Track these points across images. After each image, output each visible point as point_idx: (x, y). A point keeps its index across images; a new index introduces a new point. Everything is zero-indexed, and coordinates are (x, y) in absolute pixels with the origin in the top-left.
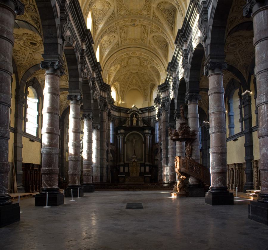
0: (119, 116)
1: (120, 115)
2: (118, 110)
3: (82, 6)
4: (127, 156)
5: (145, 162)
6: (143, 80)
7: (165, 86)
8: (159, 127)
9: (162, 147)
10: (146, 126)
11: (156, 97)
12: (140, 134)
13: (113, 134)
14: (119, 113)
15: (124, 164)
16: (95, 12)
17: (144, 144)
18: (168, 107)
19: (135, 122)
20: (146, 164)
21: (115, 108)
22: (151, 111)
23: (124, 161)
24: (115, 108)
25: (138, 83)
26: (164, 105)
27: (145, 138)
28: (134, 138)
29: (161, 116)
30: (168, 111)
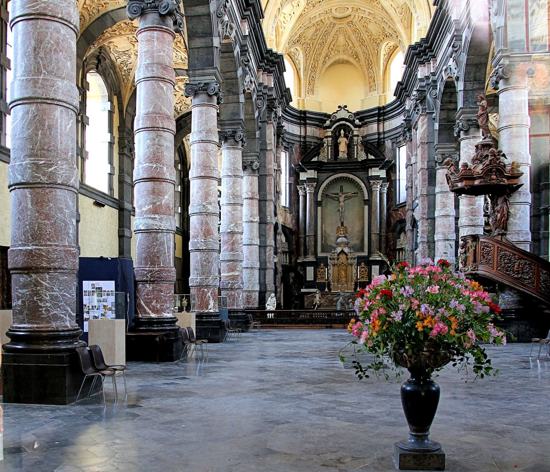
0: (303, 134)
1: (306, 133)
2: (300, 120)
6: (365, 36)
7: (426, 48)
8: (409, 159)
9: (417, 215)
10: (373, 157)
11: (400, 80)
14: (303, 129)
18: (435, 103)
19: (343, 148)
21: (293, 116)
22: (385, 117)
24: (293, 116)
25: (351, 45)
26: (425, 98)
28: (341, 190)
29: (413, 130)
30: (434, 115)
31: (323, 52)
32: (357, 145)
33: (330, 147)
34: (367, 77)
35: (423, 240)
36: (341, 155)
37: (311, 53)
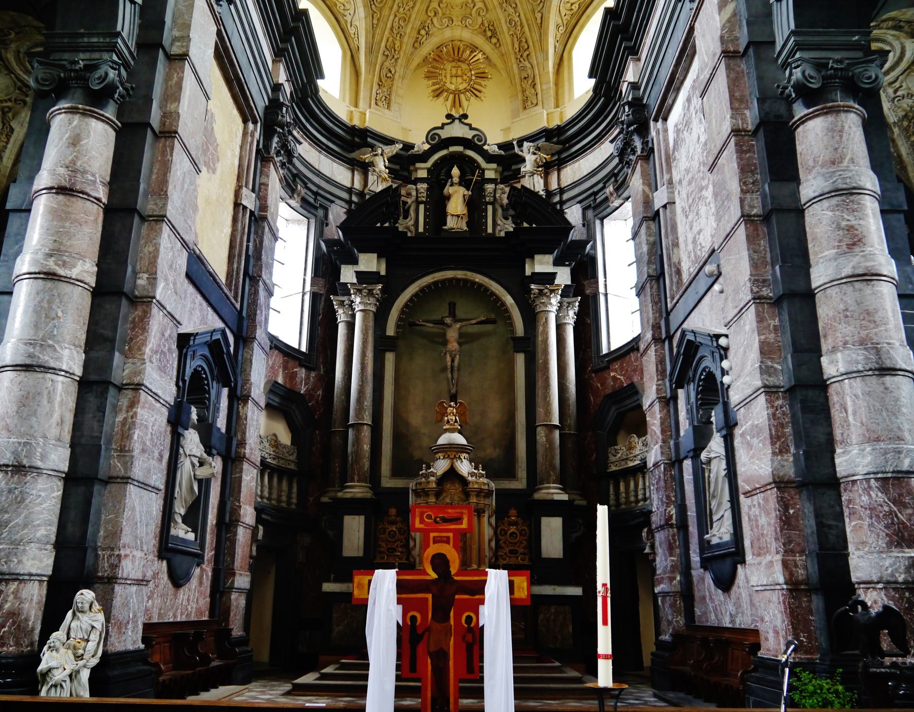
4: (399, 437)
5: (534, 481)
12: (496, 288)
13: (308, 288)
14: (358, 178)
15: (369, 495)
17: (520, 359)
20: (540, 495)
23: (374, 477)
24: (331, 134)
27: (534, 310)
28: (452, 314)
29: (655, 128)
31: (413, 16)
32: (492, 203)
33: (422, 207)
34: (518, 80)
35: (772, 381)
36: (451, 223)
37: (386, 12)
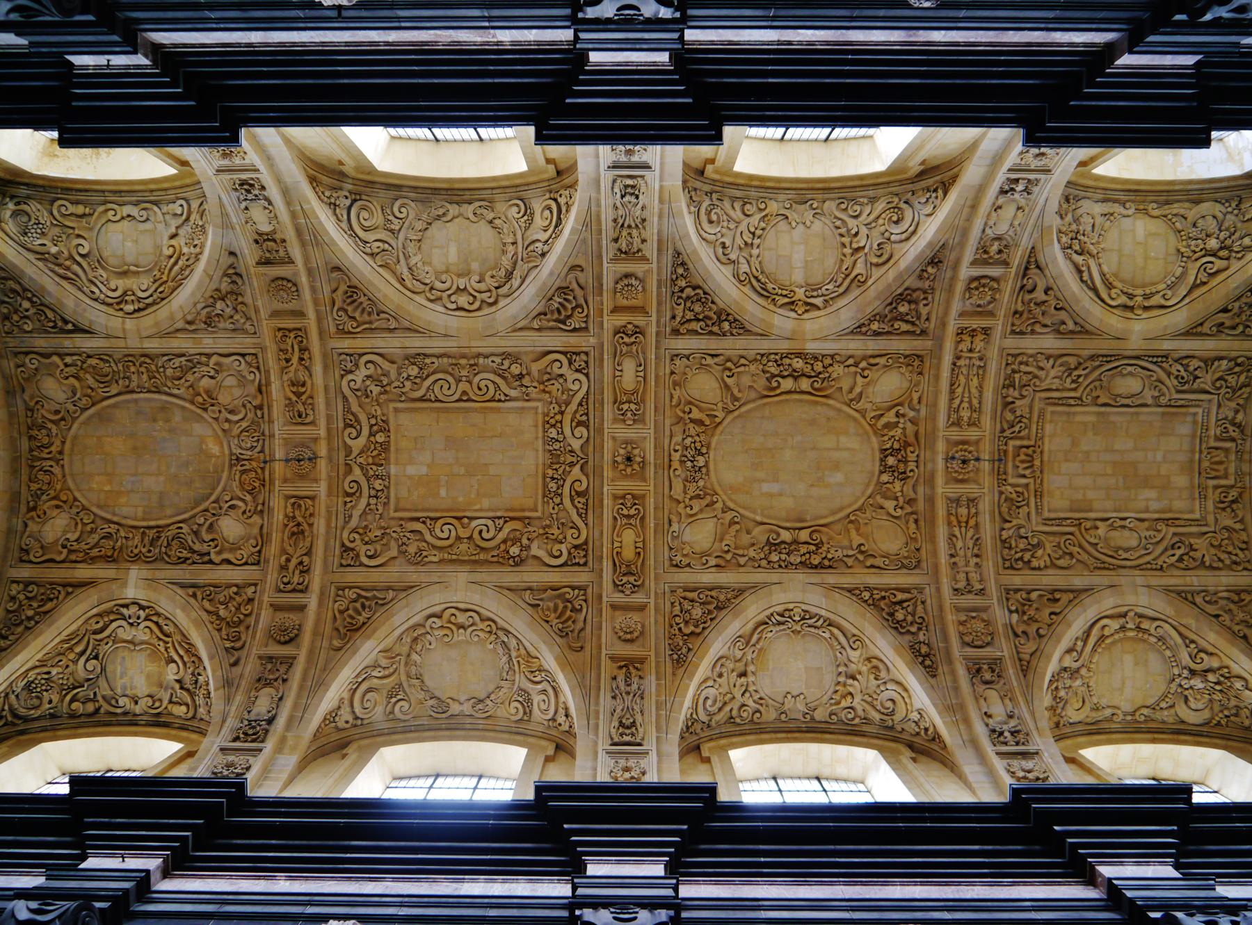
3: (288, 141)
16: (80, 209)
